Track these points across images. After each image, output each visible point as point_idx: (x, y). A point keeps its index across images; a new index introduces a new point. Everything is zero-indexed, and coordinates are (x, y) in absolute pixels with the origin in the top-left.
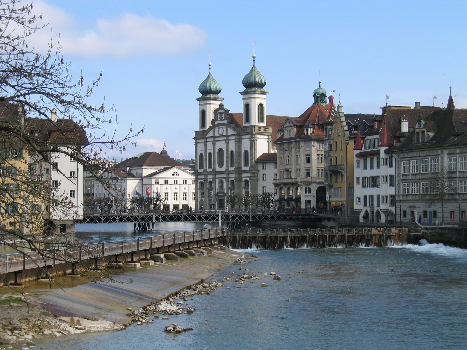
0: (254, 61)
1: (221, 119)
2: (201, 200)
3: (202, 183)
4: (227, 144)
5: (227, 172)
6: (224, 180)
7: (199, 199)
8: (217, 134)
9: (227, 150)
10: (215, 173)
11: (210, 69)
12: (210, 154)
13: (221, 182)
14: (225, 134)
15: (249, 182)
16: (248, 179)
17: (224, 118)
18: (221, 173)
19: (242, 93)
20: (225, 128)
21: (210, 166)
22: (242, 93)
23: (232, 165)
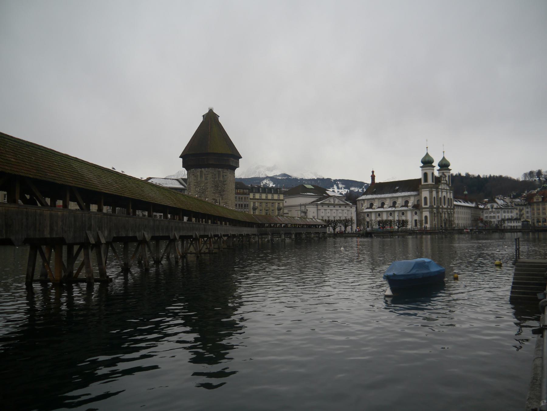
0: (444, 154)
1: (443, 181)
2: (435, 223)
3: (435, 213)
4: (447, 193)
5: (447, 208)
6: (446, 212)
7: (434, 222)
8: (443, 188)
9: (447, 197)
10: (443, 208)
11: (427, 150)
12: (440, 198)
13: (445, 213)
14: (446, 188)
15: (453, 215)
16: (452, 213)
17: (444, 180)
18: (445, 209)
19: (421, 167)
20: (446, 185)
21: (441, 205)
22: (421, 167)
23: (449, 205)
